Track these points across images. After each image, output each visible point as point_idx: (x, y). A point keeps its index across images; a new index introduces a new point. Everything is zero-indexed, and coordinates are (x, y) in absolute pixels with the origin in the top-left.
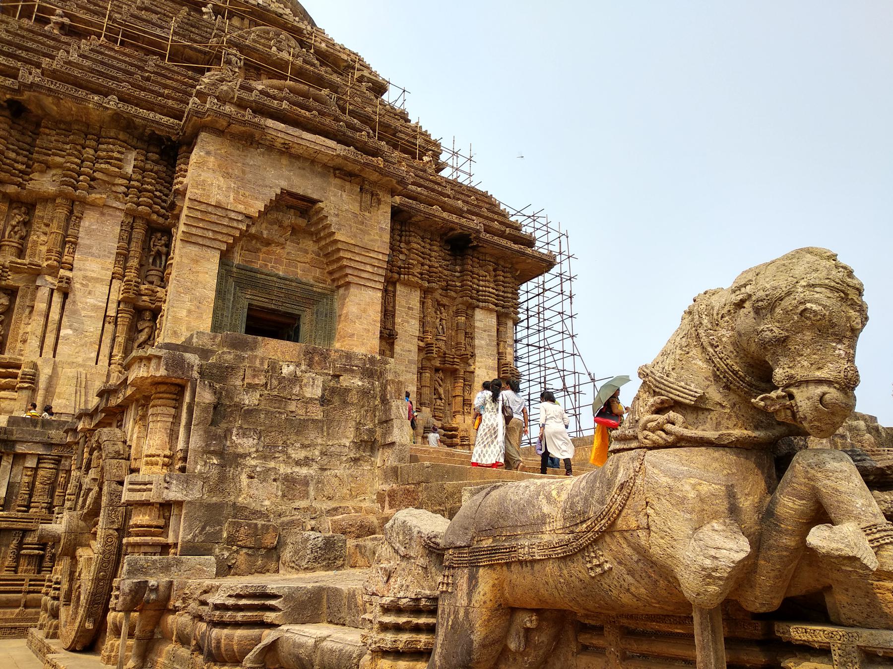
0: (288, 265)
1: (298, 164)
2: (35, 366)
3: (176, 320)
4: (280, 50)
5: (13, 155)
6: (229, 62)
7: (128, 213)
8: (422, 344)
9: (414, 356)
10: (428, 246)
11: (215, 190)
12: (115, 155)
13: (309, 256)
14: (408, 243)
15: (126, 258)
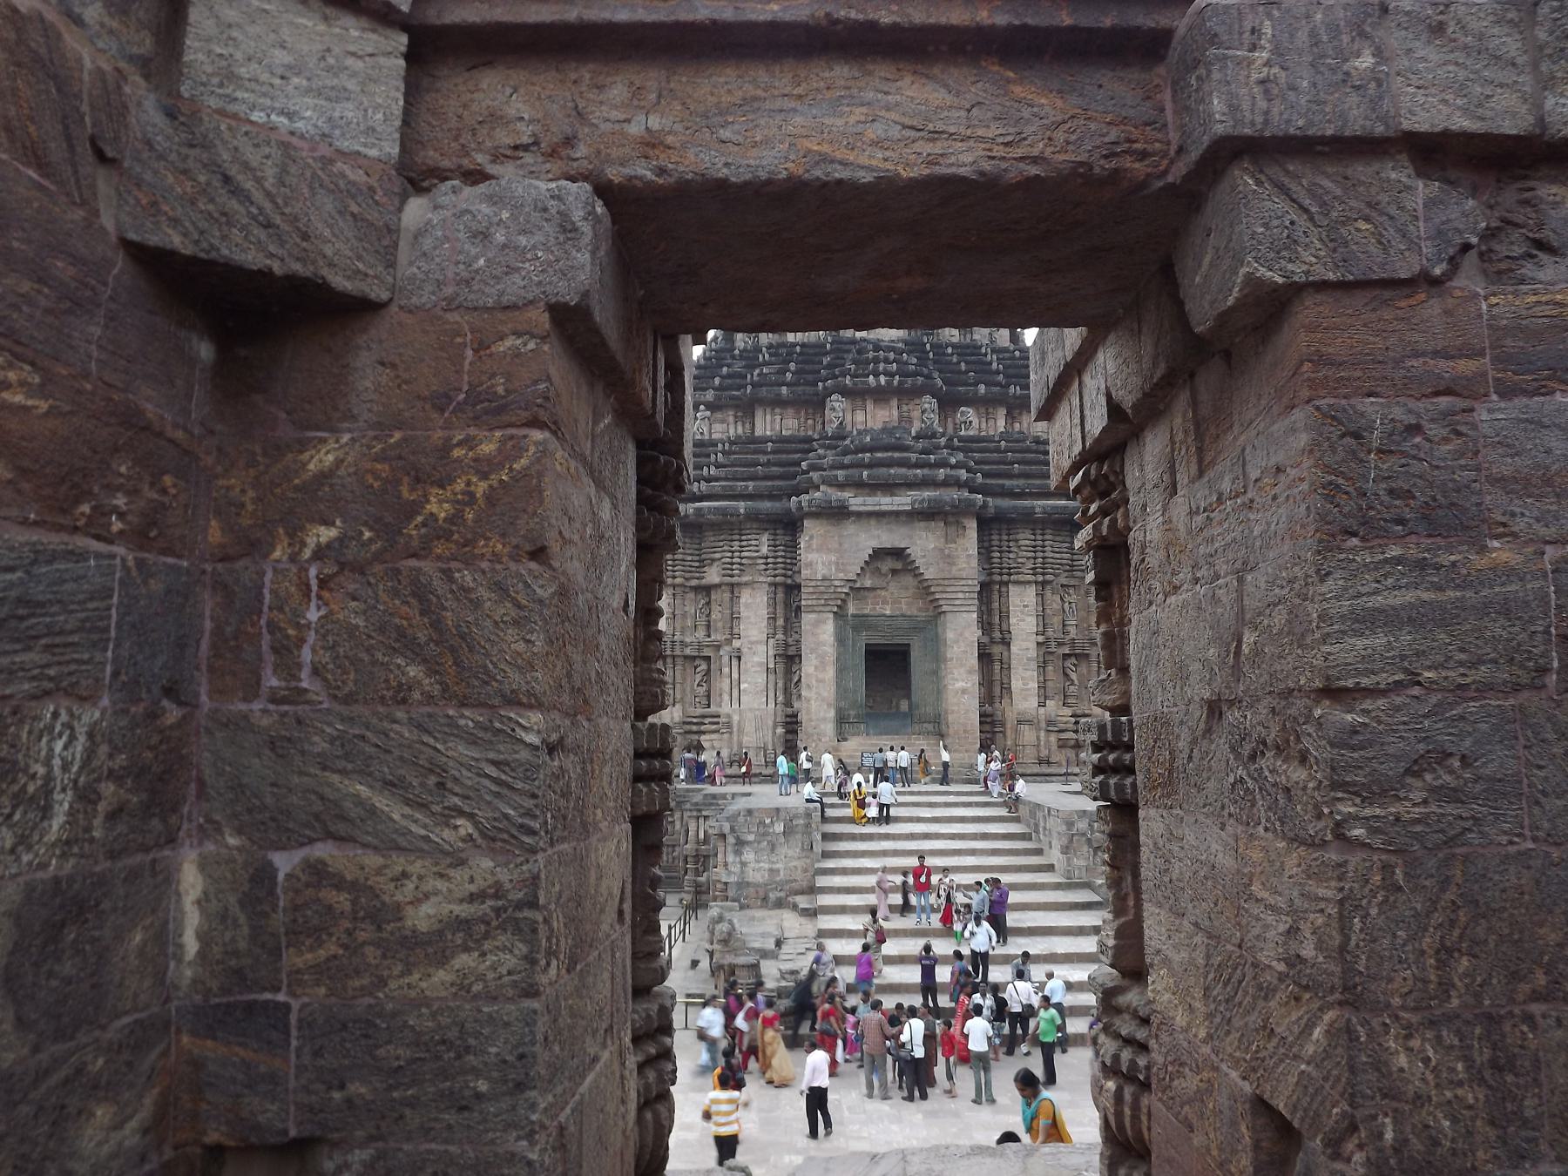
0: (894, 603)
1: (885, 521)
2: (729, 716)
3: (808, 675)
4: (876, 375)
5: (689, 558)
6: (833, 409)
7: (770, 584)
8: (1041, 638)
9: (1033, 653)
10: (1039, 537)
11: (820, 567)
12: (753, 543)
13: (911, 591)
14: (1017, 541)
15: (775, 619)
